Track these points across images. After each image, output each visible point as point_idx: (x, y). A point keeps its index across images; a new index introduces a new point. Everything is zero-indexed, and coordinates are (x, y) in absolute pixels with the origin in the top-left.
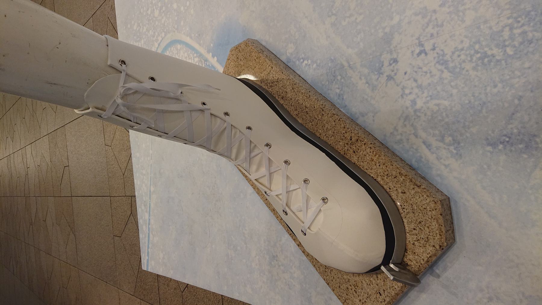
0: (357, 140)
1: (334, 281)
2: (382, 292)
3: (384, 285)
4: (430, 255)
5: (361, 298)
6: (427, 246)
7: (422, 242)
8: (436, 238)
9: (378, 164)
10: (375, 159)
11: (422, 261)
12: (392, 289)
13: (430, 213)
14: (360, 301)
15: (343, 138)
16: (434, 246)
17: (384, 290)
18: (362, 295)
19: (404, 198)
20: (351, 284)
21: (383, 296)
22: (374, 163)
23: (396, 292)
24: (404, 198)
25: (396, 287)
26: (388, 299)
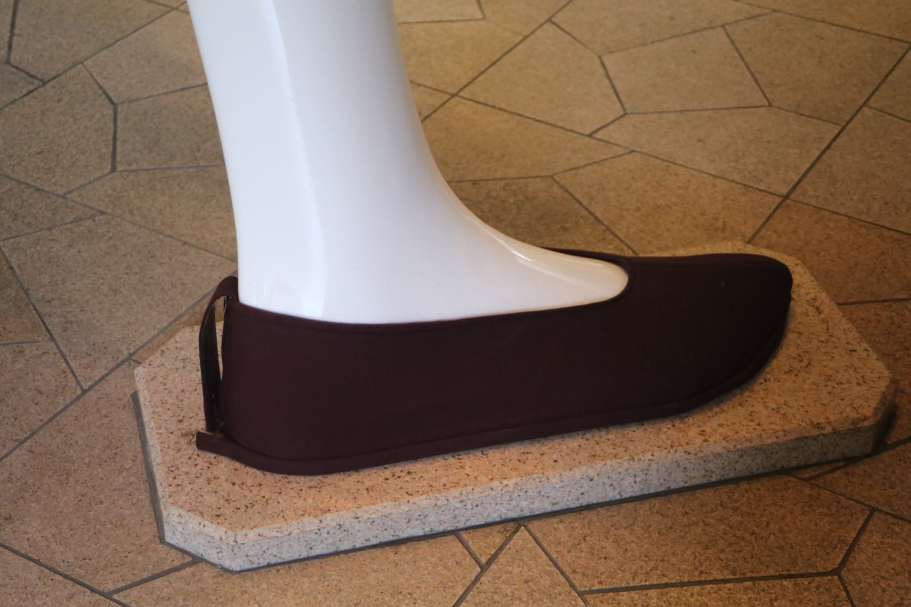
1: (808, 408)
2: (851, 347)
3: (839, 339)
5: (854, 381)
14: (859, 384)
16: (797, 265)
17: (848, 343)
21: (857, 348)
25: (846, 326)
26: (865, 345)
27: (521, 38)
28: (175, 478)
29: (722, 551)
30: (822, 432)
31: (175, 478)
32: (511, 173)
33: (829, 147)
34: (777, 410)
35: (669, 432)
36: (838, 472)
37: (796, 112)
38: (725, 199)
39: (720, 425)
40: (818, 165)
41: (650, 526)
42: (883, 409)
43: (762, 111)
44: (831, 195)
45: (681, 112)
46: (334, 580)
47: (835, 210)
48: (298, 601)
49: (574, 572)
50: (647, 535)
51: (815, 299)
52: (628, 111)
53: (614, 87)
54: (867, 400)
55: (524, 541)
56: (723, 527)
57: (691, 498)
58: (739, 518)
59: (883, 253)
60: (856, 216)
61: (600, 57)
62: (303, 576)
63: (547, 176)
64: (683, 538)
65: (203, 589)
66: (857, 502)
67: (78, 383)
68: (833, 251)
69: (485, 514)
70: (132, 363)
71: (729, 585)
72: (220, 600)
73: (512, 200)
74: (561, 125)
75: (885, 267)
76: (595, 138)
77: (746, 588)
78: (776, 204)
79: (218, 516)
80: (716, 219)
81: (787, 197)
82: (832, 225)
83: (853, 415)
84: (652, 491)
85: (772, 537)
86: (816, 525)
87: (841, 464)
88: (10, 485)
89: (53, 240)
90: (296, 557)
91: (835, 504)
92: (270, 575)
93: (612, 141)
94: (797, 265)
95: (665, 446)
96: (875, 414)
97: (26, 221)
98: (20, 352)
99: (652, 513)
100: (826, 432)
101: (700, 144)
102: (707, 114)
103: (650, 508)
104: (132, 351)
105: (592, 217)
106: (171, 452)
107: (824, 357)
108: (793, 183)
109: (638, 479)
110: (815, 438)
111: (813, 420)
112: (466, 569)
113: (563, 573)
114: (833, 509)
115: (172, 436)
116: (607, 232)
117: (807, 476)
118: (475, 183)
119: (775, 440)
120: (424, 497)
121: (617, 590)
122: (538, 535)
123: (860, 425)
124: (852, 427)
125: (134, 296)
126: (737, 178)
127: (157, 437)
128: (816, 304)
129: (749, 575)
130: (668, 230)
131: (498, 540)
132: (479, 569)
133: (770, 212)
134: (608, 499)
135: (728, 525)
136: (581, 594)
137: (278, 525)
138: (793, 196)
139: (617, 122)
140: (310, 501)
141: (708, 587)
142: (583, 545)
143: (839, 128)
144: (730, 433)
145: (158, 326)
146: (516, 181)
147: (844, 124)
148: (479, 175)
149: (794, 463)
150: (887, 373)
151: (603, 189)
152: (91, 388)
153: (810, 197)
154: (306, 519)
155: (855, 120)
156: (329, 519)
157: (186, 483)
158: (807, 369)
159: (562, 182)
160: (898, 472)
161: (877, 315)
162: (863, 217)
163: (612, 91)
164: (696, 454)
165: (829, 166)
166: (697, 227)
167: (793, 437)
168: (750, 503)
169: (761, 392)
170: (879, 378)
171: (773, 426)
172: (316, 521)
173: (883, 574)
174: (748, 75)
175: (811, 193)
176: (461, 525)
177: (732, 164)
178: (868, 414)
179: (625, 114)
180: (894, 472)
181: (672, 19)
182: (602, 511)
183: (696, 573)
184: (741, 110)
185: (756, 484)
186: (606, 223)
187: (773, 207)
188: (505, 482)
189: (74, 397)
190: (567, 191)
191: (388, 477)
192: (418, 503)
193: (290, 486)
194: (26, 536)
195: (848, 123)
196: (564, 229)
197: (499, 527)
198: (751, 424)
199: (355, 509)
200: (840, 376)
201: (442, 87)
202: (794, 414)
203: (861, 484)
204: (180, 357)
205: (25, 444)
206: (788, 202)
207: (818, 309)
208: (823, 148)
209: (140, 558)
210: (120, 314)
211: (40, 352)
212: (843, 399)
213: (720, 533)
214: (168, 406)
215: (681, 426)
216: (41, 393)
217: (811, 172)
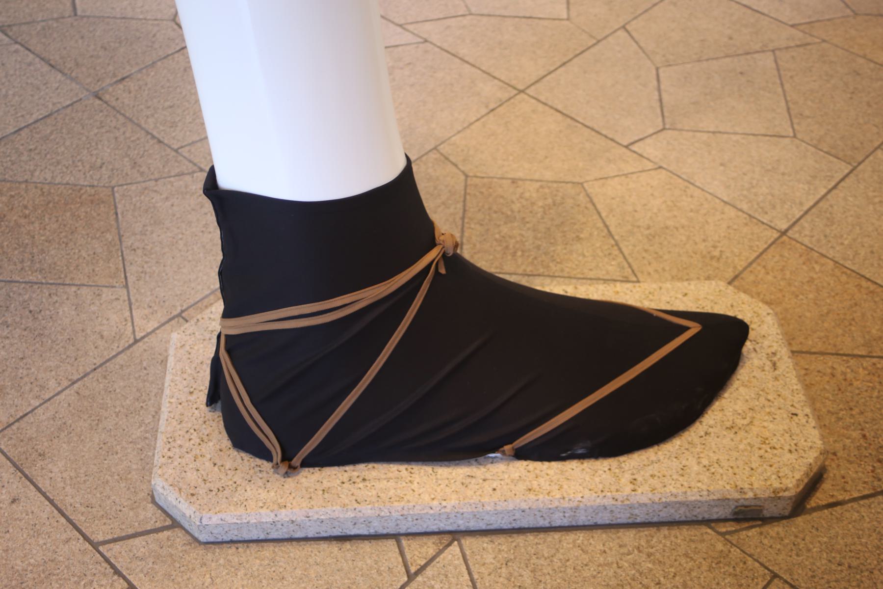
1: (736, 471)
2: (794, 411)
3: (785, 399)
5: (787, 447)
7: (756, 320)
9: (628, 292)
14: (790, 451)
16: (768, 314)
17: (792, 406)
18: (783, 442)
20: (757, 446)
22: (622, 294)
25: (795, 387)
26: (808, 410)
27: (594, 41)
28: (169, 450)
30: (743, 496)
31: (169, 450)
32: (548, 175)
33: (835, 187)
34: (707, 468)
35: (604, 476)
36: (754, 530)
37: (815, 147)
38: (728, 227)
39: (651, 476)
40: (821, 204)
41: (568, 560)
42: (806, 481)
43: (787, 141)
44: (826, 236)
45: (714, 132)
46: (281, 567)
47: (824, 252)
48: (245, 583)
50: (563, 569)
51: (774, 354)
52: (667, 126)
53: (661, 100)
54: (793, 470)
55: (454, 556)
56: (633, 572)
57: (614, 536)
58: (650, 566)
59: (856, 304)
60: (841, 262)
61: (657, 69)
62: (256, 558)
63: (578, 183)
64: (594, 577)
65: (171, 555)
66: (762, 564)
67: (134, 331)
68: (811, 296)
69: (425, 526)
70: (181, 320)
72: (182, 569)
73: (540, 204)
74: (604, 132)
75: (853, 319)
76: (630, 150)
78: (772, 239)
79: (193, 495)
80: (715, 247)
81: (784, 233)
82: (817, 268)
83: (776, 485)
84: (580, 523)
86: (718, 584)
87: (760, 523)
88: (52, 422)
89: (156, 191)
90: (255, 538)
91: (741, 565)
92: (230, 551)
93: (645, 155)
94: (768, 314)
95: (596, 490)
96: (798, 486)
97: (142, 170)
98: (99, 295)
99: (574, 546)
100: (747, 497)
101: (722, 168)
102: (734, 138)
103: (574, 541)
104: (184, 308)
105: (606, 231)
106: (175, 423)
107: (767, 418)
108: (794, 220)
109: (567, 515)
110: (737, 501)
111: (738, 483)
112: (396, 576)
115: (180, 406)
116: (616, 248)
117: (724, 530)
118: (514, 181)
119: (699, 498)
120: (369, 506)
122: (468, 553)
123: (781, 494)
124: (773, 495)
125: (201, 255)
126: (745, 207)
127: (168, 405)
128: (775, 359)
130: (669, 252)
131: (431, 551)
132: (406, 579)
133: (766, 246)
134: (538, 526)
135: (638, 571)
137: (239, 514)
138: (790, 233)
139: (654, 136)
140: (272, 494)
142: (504, 570)
143: (850, 168)
144: (659, 486)
145: (212, 287)
146: (550, 184)
147: (855, 164)
148: (520, 174)
149: (715, 517)
150: (819, 443)
151: (624, 202)
152: (143, 338)
153: (806, 236)
154: (263, 511)
155: (867, 161)
156: (283, 514)
157: (177, 456)
158: (747, 428)
159: (590, 191)
160: (808, 538)
161: (833, 368)
162: (848, 264)
163: (658, 104)
164: (622, 502)
165: (831, 206)
166: (696, 253)
167: (715, 498)
168: (664, 551)
169: (699, 446)
170: (811, 447)
171: (699, 485)
172: (272, 515)
174: (783, 104)
175: (807, 233)
176: (402, 531)
177: (745, 192)
178: (790, 485)
179: (664, 129)
181: (731, 38)
182: (531, 537)
184: (767, 138)
185: (675, 531)
186: (616, 237)
187: (770, 242)
188: (444, 503)
189: (127, 345)
190: (591, 201)
191: (345, 480)
192: (363, 511)
193: (260, 475)
194: (51, 475)
195: (860, 164)
196: (578, 239)
197: (435, 538)
198: (681, 479)
199: (307, 509)
200: (775, 440)
201: (513, 83)
203: (771, 547)
204: (210, 329)
205: (76, 386)
206: (785, 238)
207: (774, 364)
208: (830, 187)
209: (131, 513)
210: (185, 271)
211: (114, 297)
212: (771, 466)
213: (628, 578)
214: (185, 376)
215: (617, 471)
216: (102, 337)
217: (814, 210)
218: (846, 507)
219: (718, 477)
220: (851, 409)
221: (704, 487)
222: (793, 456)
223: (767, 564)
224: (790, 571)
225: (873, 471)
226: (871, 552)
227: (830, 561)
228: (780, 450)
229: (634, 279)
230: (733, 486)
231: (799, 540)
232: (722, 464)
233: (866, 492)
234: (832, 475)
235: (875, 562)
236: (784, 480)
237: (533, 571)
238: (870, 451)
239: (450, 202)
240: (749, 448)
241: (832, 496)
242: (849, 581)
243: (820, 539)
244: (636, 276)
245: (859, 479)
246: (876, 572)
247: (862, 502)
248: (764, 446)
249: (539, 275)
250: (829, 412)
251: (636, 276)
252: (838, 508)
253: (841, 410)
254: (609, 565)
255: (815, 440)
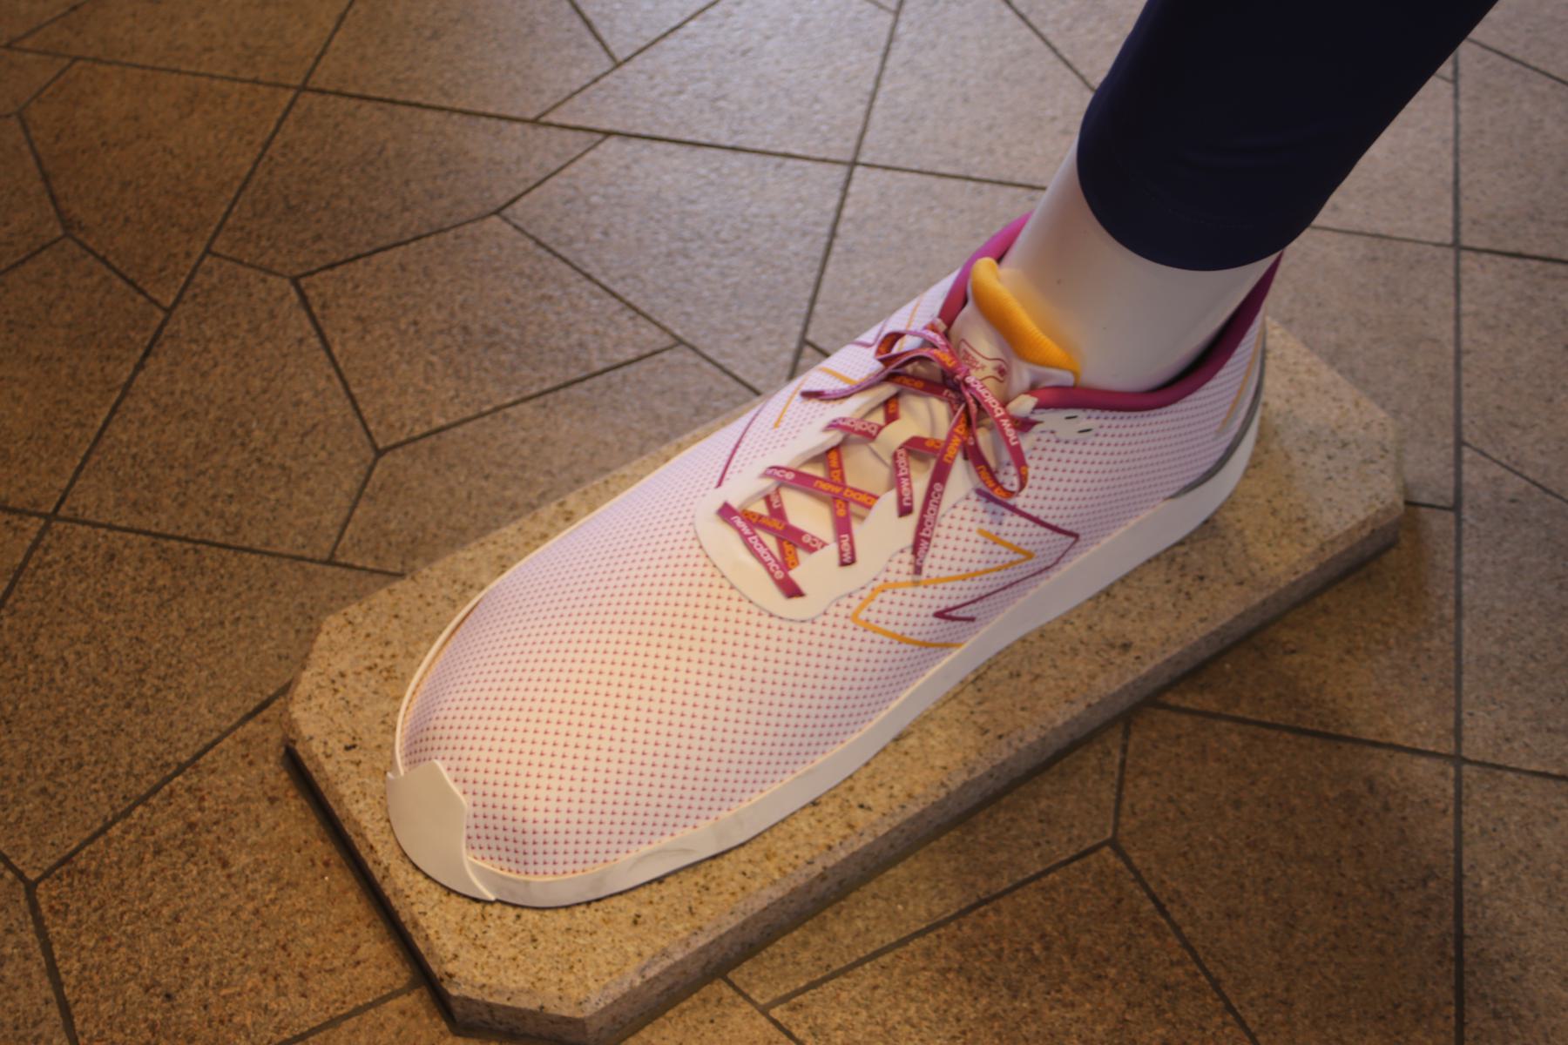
0: (851, 826)
1: (420, 603)
2: (354, 755)
4: (433, 937)
5: (350, 680)
6: (461, 939)
7: (476, 928)
8: (477, 972)
10: (771, 866)
11: (421, 908)
12: (358, 789)
13: (554, 977)
14: (342, 675)
15: (877, 781)
16: (456, 957)
17: (358, 763)
18: (359, 687)
19: (621, 917)
20: (400, 659)
21: (343, 756)
22: (758, 857)
23: (346, 800)
24: (621, 917)
25: (361, 805)
29: (524, 441)
49: (697, 365)
64: (577, 445)
71: (509, 400)
77: (489, 402)
85: (462, 479)
86: (406, 514)
91: (381, 553)
111: (412, 584)
113: (709, 360)
114: (384, 544)
121: (640, 358)
129: (487, 419)
132: (810, 337)
136: (679, 342)
141: (534, 390)
160: (292, 635)
170: (310, 698)
171: (469, 555)
173: (323, 469)
180: (298, 631)
183: (551, 403)
198: (501, 551)
200: (372, 682)
202: (441, 586)
218: (241, 714)
219: (445, 580)
220: (256, 912)
221: (461, 554)
222: (333, 672)
223: (344, 571)
224: (308, 577)
225: (202, 799)
226: (191, 660)
227: (253, 618)
228: (359, 669)
229: (776, 1013)
230: (418, 578)
231: (305, 627)
232: (446, 602)
233: (209, 756)
234: (271, 758)
235: (184, 647)
236: (342, 621)
237: (658, 417)
238: (211, 837)
239: (1278, 1017)
240: (411, 649)
241: (265, 721)
242: (221, 602)
243: (272, 644)
244: (775, 1022)
245: (224, 773)
246: (181, 633)
247: (215, 735)
248: (388, 663)
249: (963, 913)
250: (296, 885)
251: (775, 1022)
252: (252, 705)
253: (273, 901)
254: (564, 469)
255: (306, 715)
